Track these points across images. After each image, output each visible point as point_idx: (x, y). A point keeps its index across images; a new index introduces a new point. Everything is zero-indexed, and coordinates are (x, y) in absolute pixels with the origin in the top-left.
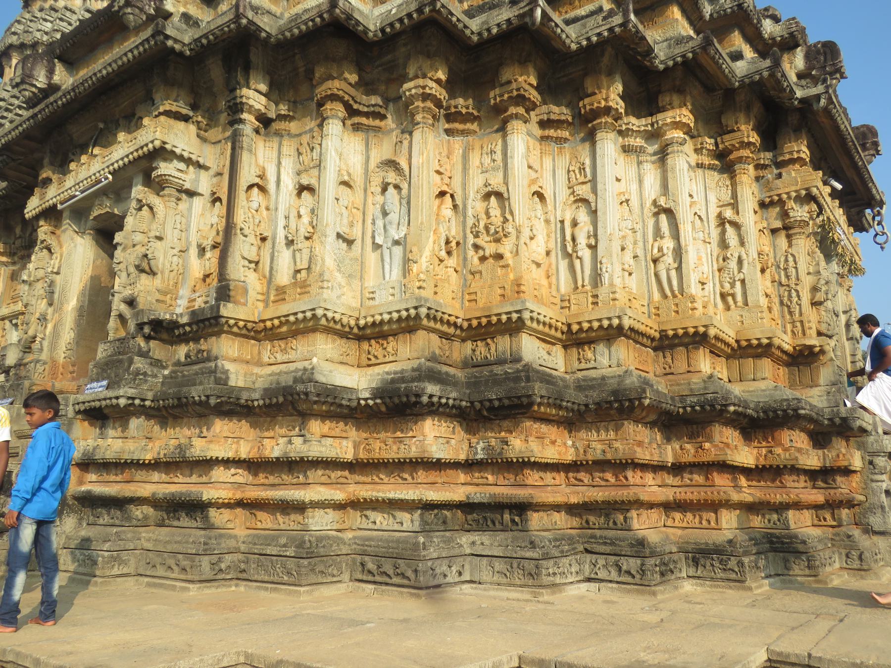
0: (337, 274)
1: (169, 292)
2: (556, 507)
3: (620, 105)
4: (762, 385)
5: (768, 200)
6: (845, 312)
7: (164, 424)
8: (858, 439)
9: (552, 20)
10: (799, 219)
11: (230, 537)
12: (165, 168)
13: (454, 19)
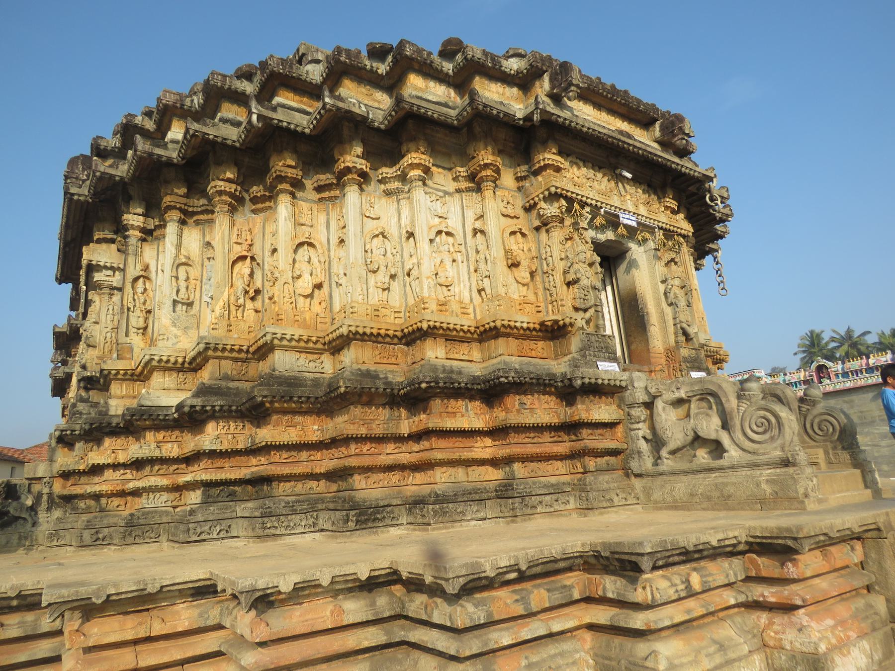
0: (173, 329)
3: (362, 164)
5: (528, 204)
6: (663, 282)
8: (619, 394)
9: (274, 119)
10: (549, 215)
11: (116, 516)
12: (98, 277)
13: (211, 137)
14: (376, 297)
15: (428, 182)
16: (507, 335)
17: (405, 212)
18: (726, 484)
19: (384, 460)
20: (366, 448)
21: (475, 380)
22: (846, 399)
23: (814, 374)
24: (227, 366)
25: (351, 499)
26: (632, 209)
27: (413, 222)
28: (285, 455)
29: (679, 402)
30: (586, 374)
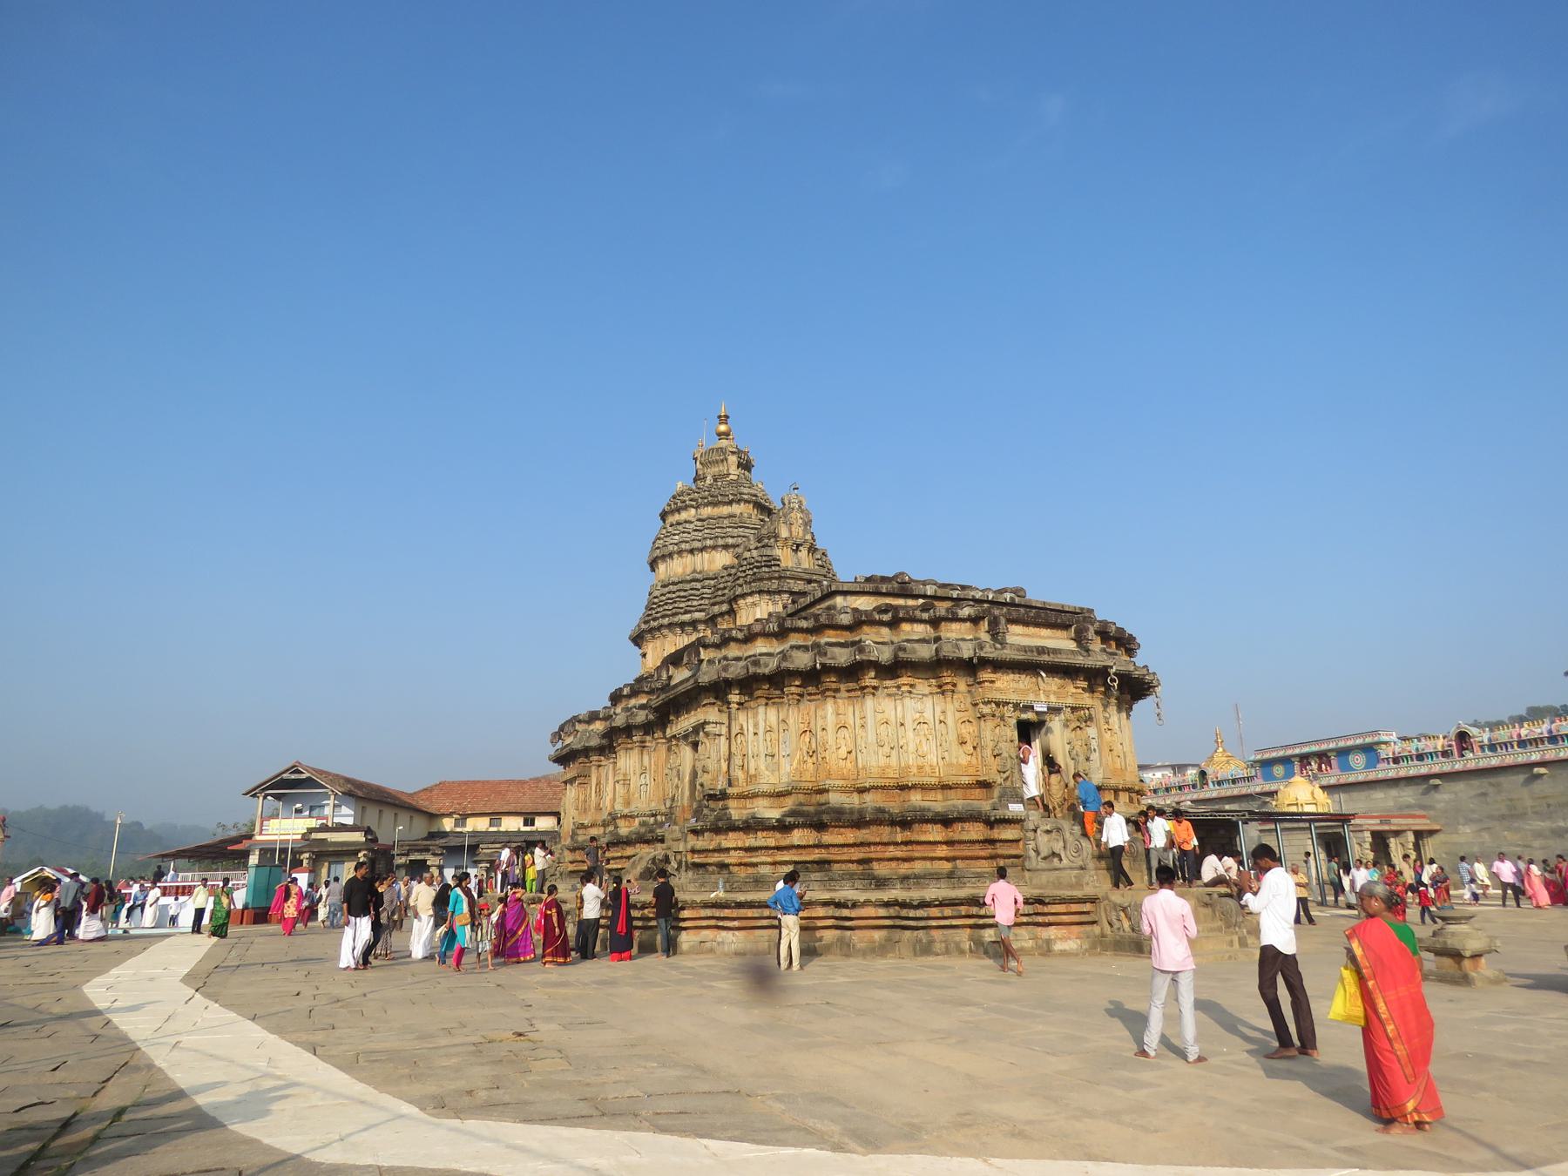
1: (715, 779)
2: (851, 862)
3: (875, 683)
4: (949, 803)
7: (717, 834)
12: (708, 728)
14: (883, 761)
15: (914, 691)
16: (957, 788)
17: (899, 709)
18: (1061, 877)
19: (888, 855)
20: (879, 848)
21: (937, 814)
22: (1493, 780)
23: (1454, 743)
24: (801, 798)
25: (873, 874)
26: (1043, 700)
27: (903, 717)
28: (837, 849)
29: (1048, 832)
30: (1000, 814)
